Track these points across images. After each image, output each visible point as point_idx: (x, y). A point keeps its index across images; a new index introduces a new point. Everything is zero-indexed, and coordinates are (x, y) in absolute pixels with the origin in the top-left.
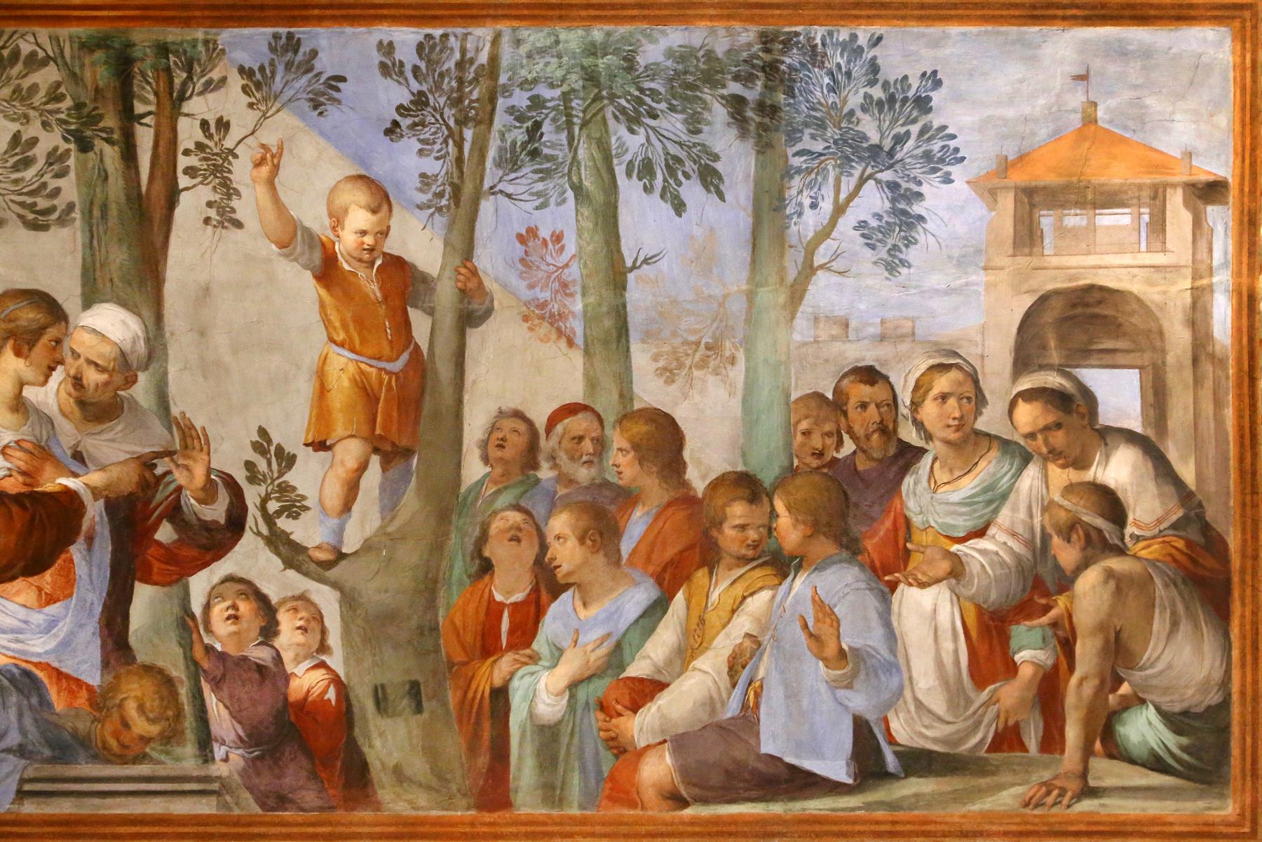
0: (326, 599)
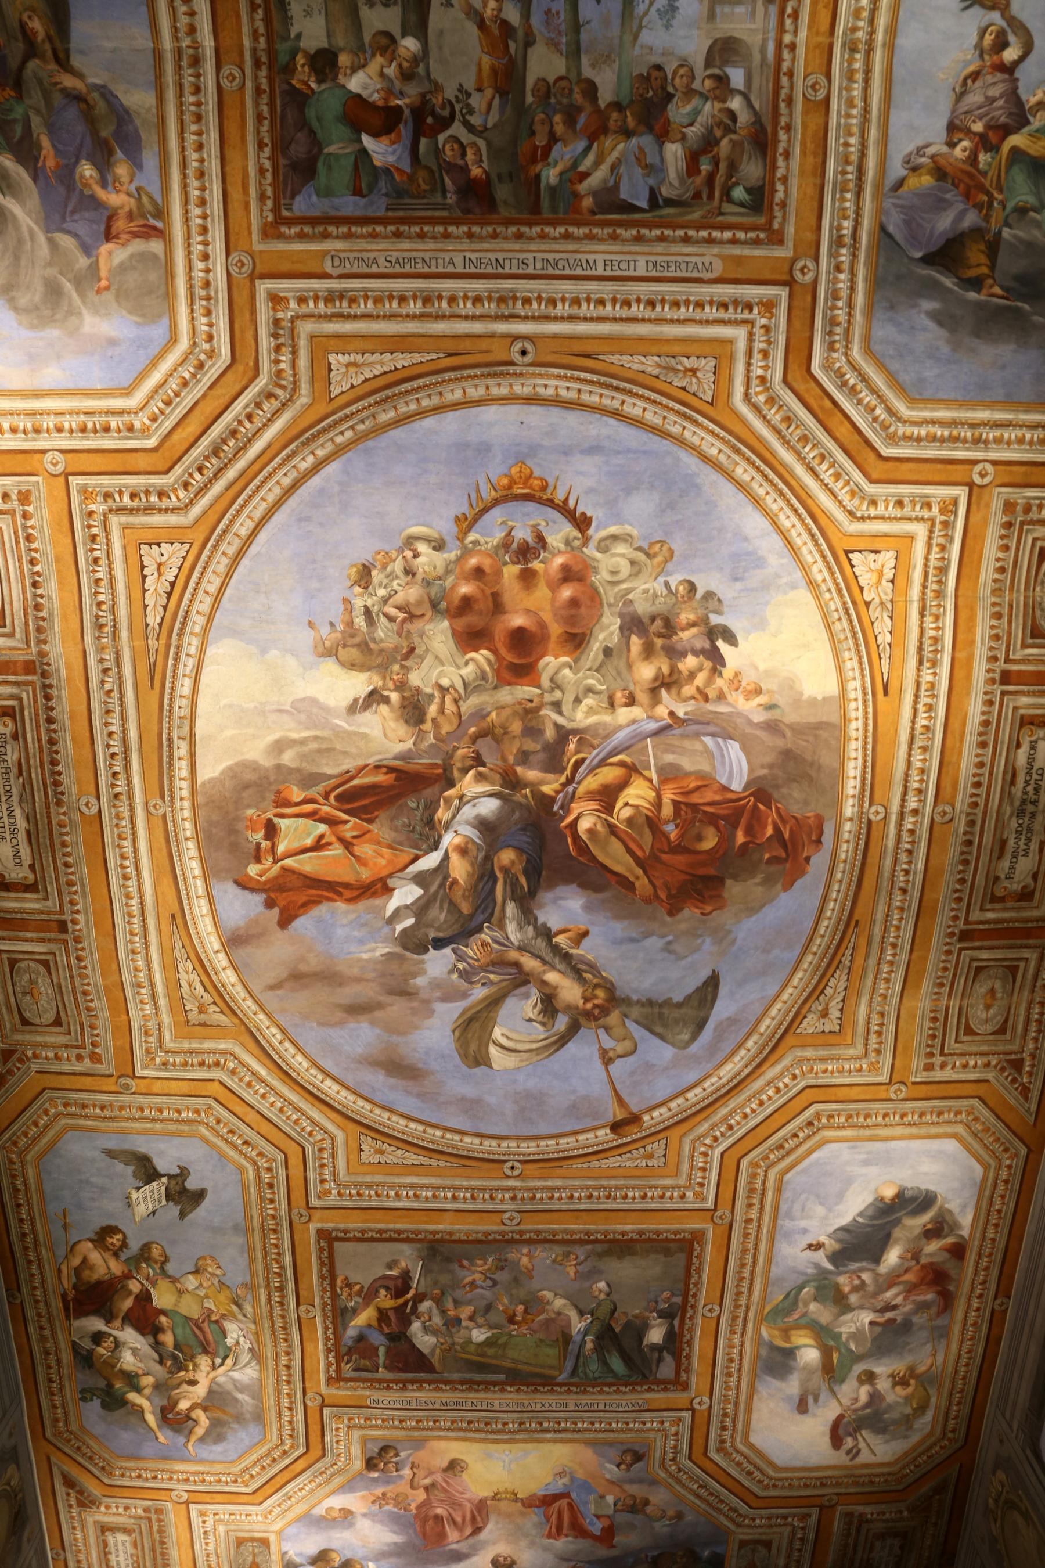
0: (482, 144)
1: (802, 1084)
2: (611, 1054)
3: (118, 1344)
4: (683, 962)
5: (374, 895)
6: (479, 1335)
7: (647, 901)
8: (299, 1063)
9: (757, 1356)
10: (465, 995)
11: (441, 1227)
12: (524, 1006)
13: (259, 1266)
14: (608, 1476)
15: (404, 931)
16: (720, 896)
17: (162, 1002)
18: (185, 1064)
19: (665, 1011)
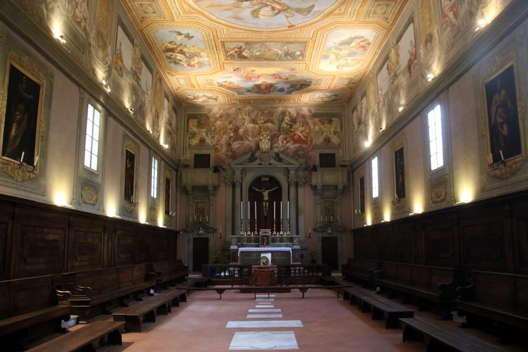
6: (258, 54)
8: (214, 18)
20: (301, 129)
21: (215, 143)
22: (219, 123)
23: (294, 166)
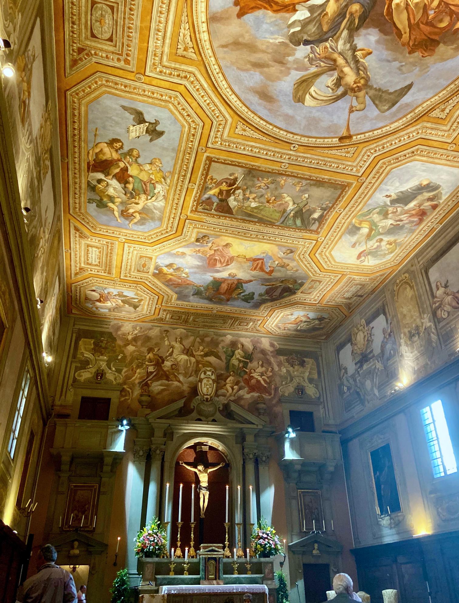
1: (419, 137)
2: (354, 109)
3: (108, 185)
4: (403, 76)
5: (288, 11)
6: (253, 205)
7: (403, 45)
8: (223, 84)
9: (347, 227)
10: (307, 69)
11: (257, 164)
12: (329, 80)
13: (178, 166)
14: (279, 256)
15: (294, 33)
16: (434, 50)
17: (168, 41)
18: (171, 74)
19: (383, 95)
20: (260, 370)
21: (121, 381)
22: (131, 348)
23: (255, 426)
